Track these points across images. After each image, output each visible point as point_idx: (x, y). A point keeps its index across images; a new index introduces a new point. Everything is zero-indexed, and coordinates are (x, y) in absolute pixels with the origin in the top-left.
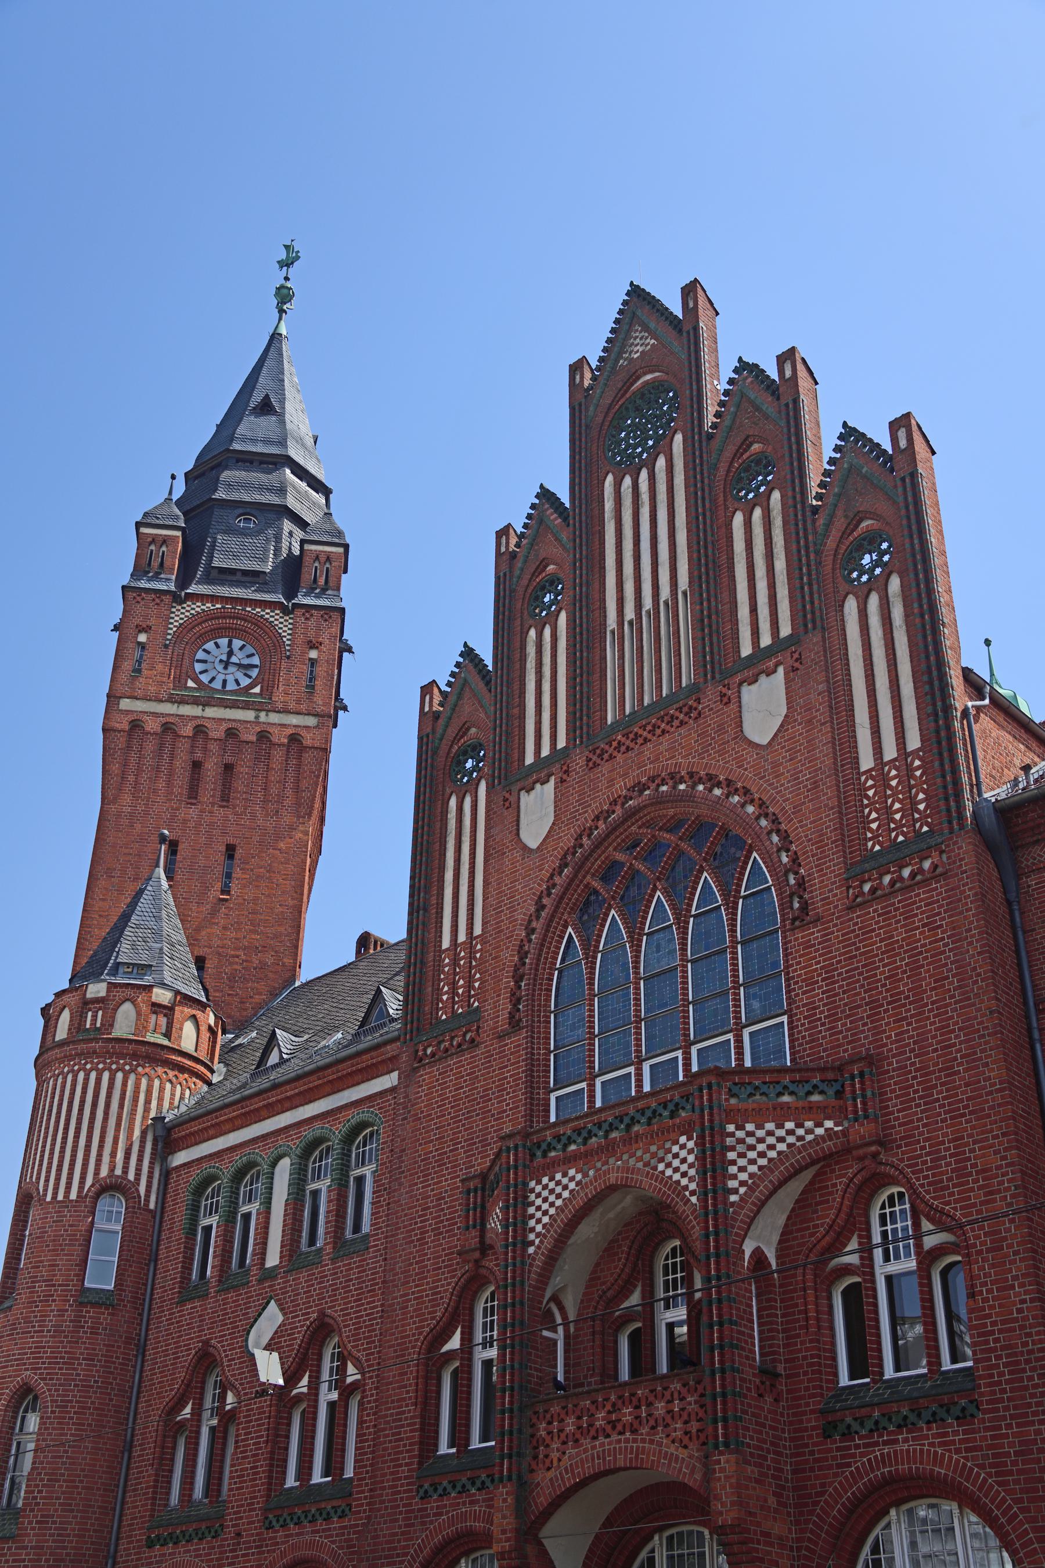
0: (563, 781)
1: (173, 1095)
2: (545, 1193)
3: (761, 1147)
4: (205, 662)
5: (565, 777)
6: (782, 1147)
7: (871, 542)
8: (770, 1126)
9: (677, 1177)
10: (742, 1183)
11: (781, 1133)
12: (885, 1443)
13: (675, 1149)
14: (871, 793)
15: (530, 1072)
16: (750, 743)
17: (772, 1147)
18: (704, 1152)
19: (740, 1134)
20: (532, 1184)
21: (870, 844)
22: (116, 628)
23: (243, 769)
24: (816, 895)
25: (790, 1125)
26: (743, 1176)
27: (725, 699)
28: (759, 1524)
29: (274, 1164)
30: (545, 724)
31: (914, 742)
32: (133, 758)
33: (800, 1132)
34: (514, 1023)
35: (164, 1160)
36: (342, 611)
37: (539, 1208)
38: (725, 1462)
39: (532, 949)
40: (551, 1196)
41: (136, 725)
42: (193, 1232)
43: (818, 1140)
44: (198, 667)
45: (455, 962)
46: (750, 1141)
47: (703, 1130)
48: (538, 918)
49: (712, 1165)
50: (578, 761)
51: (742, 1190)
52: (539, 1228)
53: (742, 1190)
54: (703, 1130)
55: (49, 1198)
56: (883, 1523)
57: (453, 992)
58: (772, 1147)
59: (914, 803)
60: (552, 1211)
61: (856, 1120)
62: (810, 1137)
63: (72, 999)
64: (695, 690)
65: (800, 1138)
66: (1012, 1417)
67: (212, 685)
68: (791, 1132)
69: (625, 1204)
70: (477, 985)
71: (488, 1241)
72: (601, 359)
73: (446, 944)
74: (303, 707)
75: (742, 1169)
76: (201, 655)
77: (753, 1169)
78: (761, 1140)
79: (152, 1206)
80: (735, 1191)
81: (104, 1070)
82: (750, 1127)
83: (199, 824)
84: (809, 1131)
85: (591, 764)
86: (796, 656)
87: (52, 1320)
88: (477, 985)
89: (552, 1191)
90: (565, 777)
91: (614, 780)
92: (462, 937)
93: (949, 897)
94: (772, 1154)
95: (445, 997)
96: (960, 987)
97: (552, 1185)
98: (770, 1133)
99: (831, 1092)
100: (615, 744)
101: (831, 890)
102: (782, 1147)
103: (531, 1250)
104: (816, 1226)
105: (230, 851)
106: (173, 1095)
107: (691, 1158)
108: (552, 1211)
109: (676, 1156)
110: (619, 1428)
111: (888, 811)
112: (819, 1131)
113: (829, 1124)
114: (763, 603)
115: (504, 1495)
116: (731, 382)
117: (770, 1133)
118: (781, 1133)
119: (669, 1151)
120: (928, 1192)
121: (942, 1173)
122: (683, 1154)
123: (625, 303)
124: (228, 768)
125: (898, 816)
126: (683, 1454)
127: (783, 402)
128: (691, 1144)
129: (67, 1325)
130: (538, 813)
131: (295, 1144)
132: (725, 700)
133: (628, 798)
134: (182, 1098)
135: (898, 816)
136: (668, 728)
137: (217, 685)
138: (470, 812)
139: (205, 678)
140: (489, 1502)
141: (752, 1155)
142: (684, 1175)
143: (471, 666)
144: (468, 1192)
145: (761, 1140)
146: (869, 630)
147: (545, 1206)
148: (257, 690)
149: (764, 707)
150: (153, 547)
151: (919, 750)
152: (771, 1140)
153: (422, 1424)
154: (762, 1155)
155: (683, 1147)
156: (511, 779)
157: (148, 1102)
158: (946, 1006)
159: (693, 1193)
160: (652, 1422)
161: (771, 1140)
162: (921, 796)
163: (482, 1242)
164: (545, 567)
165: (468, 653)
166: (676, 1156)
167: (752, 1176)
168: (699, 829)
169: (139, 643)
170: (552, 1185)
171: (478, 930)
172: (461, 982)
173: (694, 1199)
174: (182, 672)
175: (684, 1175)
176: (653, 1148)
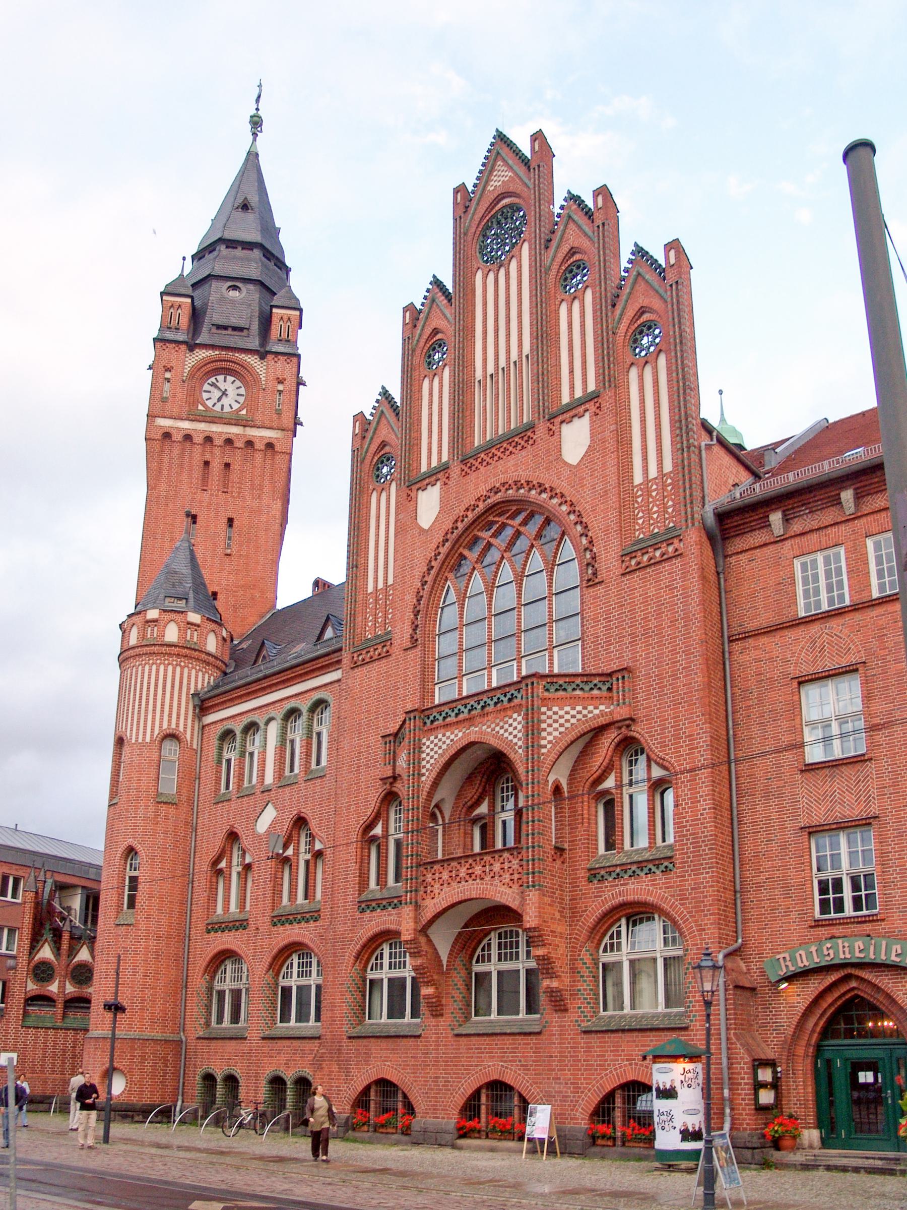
0: (445, 484)
1: (203, 680)
2: (432, 746)
3: (562, 721)
5: (447, 481)
6: (573, 721)
7: (649, 328)
8: (567, 708)
9: (511, 737)
10: (549, 742)
11: (573, 712)
12: (622, 885)
13: (511, 721)
14: (639, 500)
15: (423, 672)
16: (566, 463)
18: (527, 723)
19: (550, 713)
20: (424, 740)
21: (637, 533)
22: (150, 368)
23: (235, 467)
24: (601, 566)
26: (550, 738)
27: (551, 432)
28: (549, 927)
29: (267, 723)
30: (434, 447)
31: (668, 467)
32: (166, 459)
33: (585, 712)
34: (414, 641)
35: (200, 720)
36: (299, 356)
37: (428, 754)
38: (533, 896)
39: (425, 594)
40: (437, 747)
41: (167, 435)
42: (220, 762)
43: (594, 718)
46: (555, 717)
47: (527, 710)
48: (429, 574)
49: (532, 730)
50: (455, 471)
52: (428, 766)
53: (549, 746)
54: (527, 710)
55: (133, 741)
56: (617, 925)
57: (375, 620)
59: (665, 508)
60: (436, 756)
61: (618, 705)
62: (590, 715)
63: (137, 619)
64: (531, 427)
65: (585, 716)
66: (692, 871)
67: (214, 408)
68: (579, 712)
69: (480, 753)
70: (390, 616)
71: (397, 772)
72: (475, 186)
73: (370, 589)
74: (274, 425)
75: (550, 734)
77: (556, 734)
78: (562, 717)
79: (195, 747)
80: (545, 747)
81: (160, 664)
82: (555, 709)
83: (210, 504)
84: (590, 712)
85: (464, 473)
86: (598, 405)
87: (141, 812)
88: (390, 616)
89: (436, 745)
90: (447, 481)
91: (478, 486)
92: (380, 585)
93: (682, 569)
94: (568, 725)
95: (370, 624)
96: (685, 626)
97: (436, 741)
98: (567, 713)
99: (605, 688)
100: (479, 460)
101: (611, 563)
102: (573, 721)
103: (423, 778)
104: (590, 767)
105: (230, 521)
106: (203, 680)
107: (519, 727)
108: (436, 756)
109: (511, 725)
110: (473, 877)
111: (649, 511)
112: (597, 712)
113: (602, 707)
115: (407, 911)
116: (562, 208)
117: (567, 713)
118: (573, 712)
119: (506, 722)
120: (657, 748)
121: (666, 737)
122: (515, 724)
123: (492, 144)
124: (227, 465)
125: (655, 516)
126: (509, 891)
127: (596, 224)
128: (520, 719)
129: (151, 815)
130: (429, 505)
131: (279, 713)
132: (551, 433)
134: (209, 683)
135: (655, 516)
136: (514, 450)
139: (209, 404)
140: (399, 915)
141: (556, 725)
142: (515, 736)
143: (386, 403)
144: (386, 743)
145: (562, 717)
146: (645, 392)
147: (432, 753)
148: (244, 412)
149: (575, 439)
150: (172, 310)
151: (671, 472)
152: (568, 717)
153: (360, 873)
154: (562, 725)
155: (515, 720)
156: (414, 484)
157: (189, 684)
158: (675, 637)
159: (520, 747)
160: (492, 874)
161: (568, 717)
162: (670, 503)
163: (394, 772)
164: (434, 334)
165: (385, 393)
166: (511, 725)
167: (555, 738)
169: (166, 379)
170: (436, 741)
171: (390, 582)
172: (380, 614)
173: (520, 751)
174: (193, 398)
175: (515, 736)
176: (497, 721)
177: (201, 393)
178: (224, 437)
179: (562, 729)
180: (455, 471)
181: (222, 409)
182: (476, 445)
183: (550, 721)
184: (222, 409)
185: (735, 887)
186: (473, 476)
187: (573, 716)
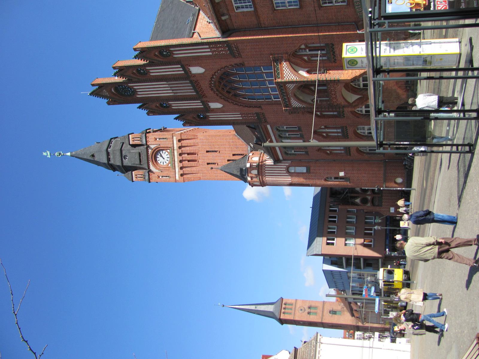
3: (288, 74)
4: (163, 163)
6: (288, 70)
8: (284, 72)
11: (285, 70)
17: (288, 72)
19: (286, 77)
25: (284, 69)
26: (294, 77)
30: (197, 104)
33: (285, 67)
44: (165, 164)
45: (245, 116)
46: (287, 75)
48: (238, 104)
51: (296, 77)
53: (296, 77)
57: (252, 116)
58: (288, 72)
62: (286, 65)
65: (286, 67)
68: (285, 69)
75: (292, 77)
76: (162, 164)
77: (292, 75)
78: (287, 74)
80: (296, 78)
84: (285, 65)
91: (210, 93)
94: (289, 72)
98: (286, 72)
102: (288, 70)
114: (177, 70)
117: (286, 72)
118: (285, 70)
119: (289, 87)
130: (214, 105)
133: (214, 91)
137: (169, 159)
138: (212, 117)
139: (167, 162)
141: (290, 75)
145: (287, 74)
152: (287, 72)
154: (290, 74)
156: (207, 109)
161: (287, 72)
167: (293, 75)
168: (221, 78)
177: (164, 165)
178: (179, 157)
179: (291, 73)
180: (205, 99)
181: (168, 158)
182: (195, 94)
183: (289, 77)
184: (168, 158)
185: (337, 25)
186: (207, 95)
187: (287, 70)
